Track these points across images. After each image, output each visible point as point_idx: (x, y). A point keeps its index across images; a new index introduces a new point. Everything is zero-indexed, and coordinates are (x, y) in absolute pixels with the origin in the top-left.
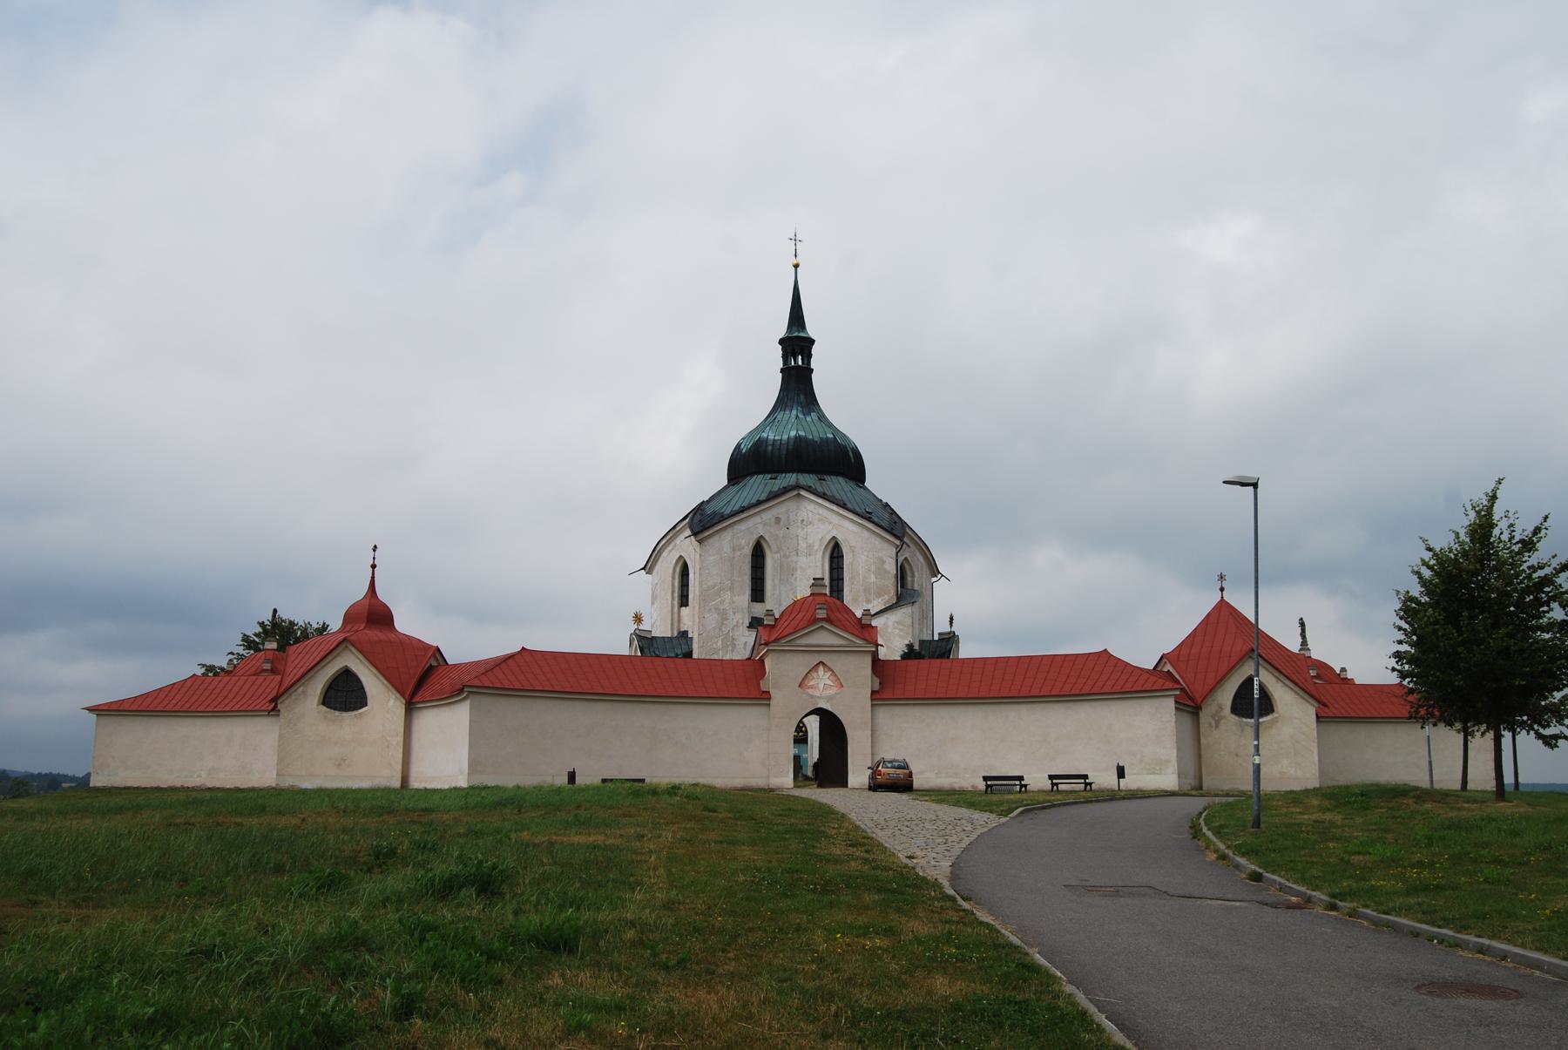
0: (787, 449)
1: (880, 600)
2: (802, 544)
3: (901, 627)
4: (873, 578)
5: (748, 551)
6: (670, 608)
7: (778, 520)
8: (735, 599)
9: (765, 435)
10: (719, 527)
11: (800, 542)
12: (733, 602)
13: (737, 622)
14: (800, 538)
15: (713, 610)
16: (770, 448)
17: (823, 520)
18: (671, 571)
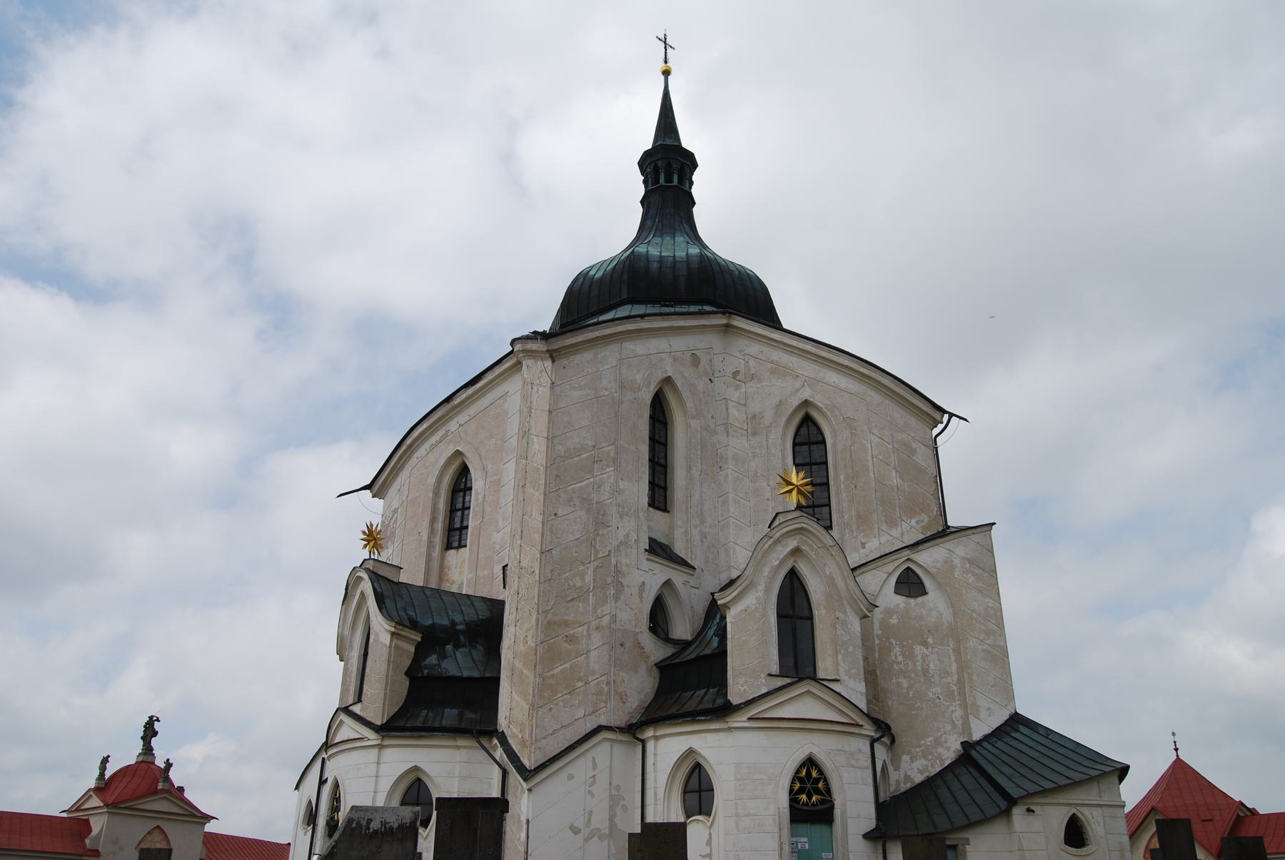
0: (689, 269)
1: (913, 522)
2: (736, 414)
3: (977, 571)
4: (894, 479)
5: (647, 396)
6: (424, 549)
7: (695, 360)
8: (622, 485)
9: (642, 249)
10: (597, 334)
11: (731, 411)
12: (620, 492)
13: (627, 536)
14: (731, 404)
15: (576, 501)
16: (655, 266)
17: (779, 371)
18: (432, 481)
